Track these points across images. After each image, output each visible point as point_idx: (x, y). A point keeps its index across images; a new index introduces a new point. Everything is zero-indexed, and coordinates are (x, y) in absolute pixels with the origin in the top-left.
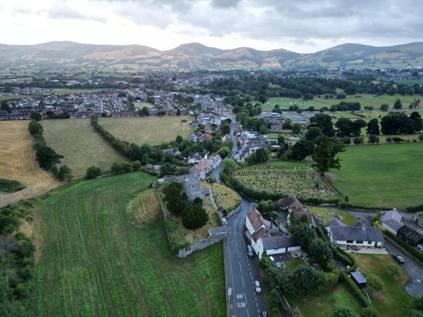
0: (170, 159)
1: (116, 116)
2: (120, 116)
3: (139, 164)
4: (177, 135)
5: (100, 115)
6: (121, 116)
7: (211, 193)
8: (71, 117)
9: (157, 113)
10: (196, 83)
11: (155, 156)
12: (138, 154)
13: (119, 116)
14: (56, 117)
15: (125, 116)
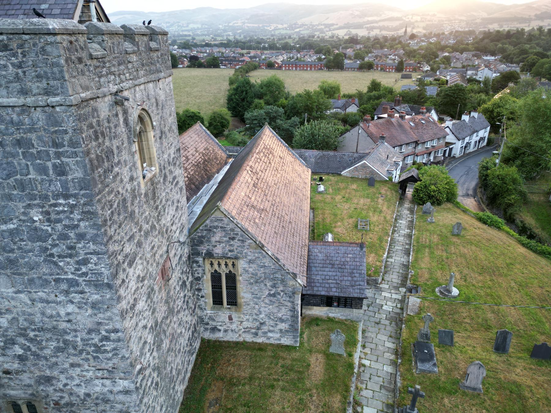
1: (289, 68)
3: (223, 118)
4: (371, 79)
6: (296, 69)
7: (394, 277)
8: (221, 67)
9: (358, 67)
10: (450, 41)
12: (243, 100)
13: (292, 68)
14: (200, 66)
15: (303, 70)
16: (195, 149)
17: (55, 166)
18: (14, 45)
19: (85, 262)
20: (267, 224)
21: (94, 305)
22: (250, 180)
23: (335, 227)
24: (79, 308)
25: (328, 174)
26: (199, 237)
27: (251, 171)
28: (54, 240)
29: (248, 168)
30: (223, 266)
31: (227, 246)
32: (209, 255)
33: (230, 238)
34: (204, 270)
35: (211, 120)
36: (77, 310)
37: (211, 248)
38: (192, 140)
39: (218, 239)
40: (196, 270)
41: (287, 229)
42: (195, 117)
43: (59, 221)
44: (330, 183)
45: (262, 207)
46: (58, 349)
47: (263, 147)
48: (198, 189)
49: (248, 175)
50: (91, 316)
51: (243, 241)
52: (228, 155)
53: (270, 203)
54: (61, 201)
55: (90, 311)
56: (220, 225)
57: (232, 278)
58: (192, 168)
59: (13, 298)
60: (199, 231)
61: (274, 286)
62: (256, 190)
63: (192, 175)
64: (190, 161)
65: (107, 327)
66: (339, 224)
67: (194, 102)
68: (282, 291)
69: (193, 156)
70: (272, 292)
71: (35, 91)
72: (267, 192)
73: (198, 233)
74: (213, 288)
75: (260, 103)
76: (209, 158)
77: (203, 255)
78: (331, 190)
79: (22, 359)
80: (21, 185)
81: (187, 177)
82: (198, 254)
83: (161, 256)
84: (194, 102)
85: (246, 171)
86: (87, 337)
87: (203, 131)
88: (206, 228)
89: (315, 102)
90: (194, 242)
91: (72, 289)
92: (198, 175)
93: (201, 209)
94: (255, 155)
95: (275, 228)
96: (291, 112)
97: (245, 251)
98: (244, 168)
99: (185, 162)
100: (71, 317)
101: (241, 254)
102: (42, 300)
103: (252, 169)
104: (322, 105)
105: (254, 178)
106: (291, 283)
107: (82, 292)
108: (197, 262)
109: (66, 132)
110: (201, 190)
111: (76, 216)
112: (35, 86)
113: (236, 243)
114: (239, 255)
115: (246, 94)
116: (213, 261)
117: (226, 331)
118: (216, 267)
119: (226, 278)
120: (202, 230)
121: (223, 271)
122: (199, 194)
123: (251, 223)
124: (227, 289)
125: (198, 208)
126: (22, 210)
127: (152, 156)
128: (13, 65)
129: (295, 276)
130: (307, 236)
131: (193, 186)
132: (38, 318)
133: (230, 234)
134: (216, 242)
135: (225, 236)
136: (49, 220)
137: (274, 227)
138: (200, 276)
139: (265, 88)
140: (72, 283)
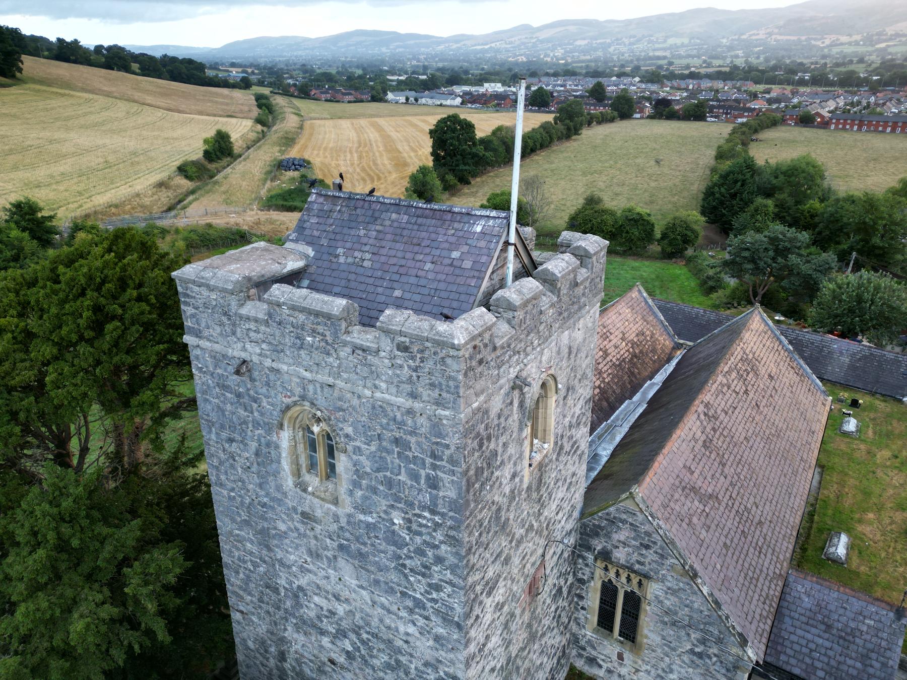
0: (876, 241)
1: (844, 126)
2: (856, 128)
3: (688, 228)
5: (791, 120)
6: (860, 129)
8: (709, 119)
11: (817, 219)
12: (733, 196)
14: (672, 116)
15: (876, 131)
16: (621, 335)
17: (428, 477)
18: (415, 349)
19: (438, 588)
20: (713, 527)
21: (437, 638)
22: (699, 433)
23: (860, 521)
24: (420, 633)
25: (873, 394)
26: (594, 525)
27: (705, 414)
28: (409, 551)
29: (701, 408)
30: (623, 579)
31: (636, 554)
32: (605, 556)
33: (641, 544)
34: (593, 574)
35: (667, 229)
36: (417, 635)
37: (609, 547)
38: (620, 318)
39: (622, 538)
40: (581, 569)
41: (750, 538)
42: (641, 222)
43: (420, 534)
44: (872, 415)
45: (710, 490)
46: (388, 666)
47: (739, 357)
48: (613, 409)
49: (698, 423)
51: (662, 556)
52: (676, 343)
53: (728, 482)
54: (426, 514)
55: (431, 643)
56: (630, 520)
57: (633, 603)
58: (610, 371)
59: (355, 591)
60: (595, 516)
61: (703, 641)
62: (708, 453)
63: (608, 383)
64: (608, 359)
65: (446, 669)
66: (871, 516)
67: (646, 186)
68: (715, 655)
69: (616, 347)
70: (697, 650)
71: (425, 398)
72: (726, 456)
73: (595, 519)
74: (601, 602)
75: (766, 206)
76: (641, 352)
77: (596, 552)
78: (870, 433)
79: (349, 656)
80: (389, 483)
81: (599, 387)
82: (589, 548)
83: (533, 564)
84: (646, 186)
85: (696, 415)
86: (422, 668)
87: (642, 299)
88: (607, 517)
89: (882, 218)
90: (585, 529)
91: (417, 610)
92: (616, 384)
93: (609, 452)
94: (720, 378)
95: (726, 537)
96: (827, 227)
97: (664, 572)
98: (693, 409)
99: (600, 360)
100: (409, 639)
101: (655, 573)
102: (383, 607)
103: (709, 409)
104: (896, 224)
105: (708, 430)
106: (735, 650)
108: (584, 558)
109: (447, 447)
110: (617, 412)
111: (439, 536)
112: (426, 393)
113: (650, 555)
114: (652, 573)
115: (742, 185)
116: (610, 566)
117: (609, 671)
118: (612, 575)
119: (625, 597)
120: (601, 517)
121: (623, 587)
122: (612, 418)
123: (684, 525)
124: (623, 612)
125: (605, 449)
126: (385, 508)
127: (547, 429)
128: (409, 367)
129: (744, 642)
130: (788, 555)
131: (605, 404)
132: (375, 622)
133: (643, 539)
134: (620, 541)
135: (634, 539)
136: (409, 529)
137: (725, 533)
138: (585, 578)
139: (782, 177)
140: (419, 604)
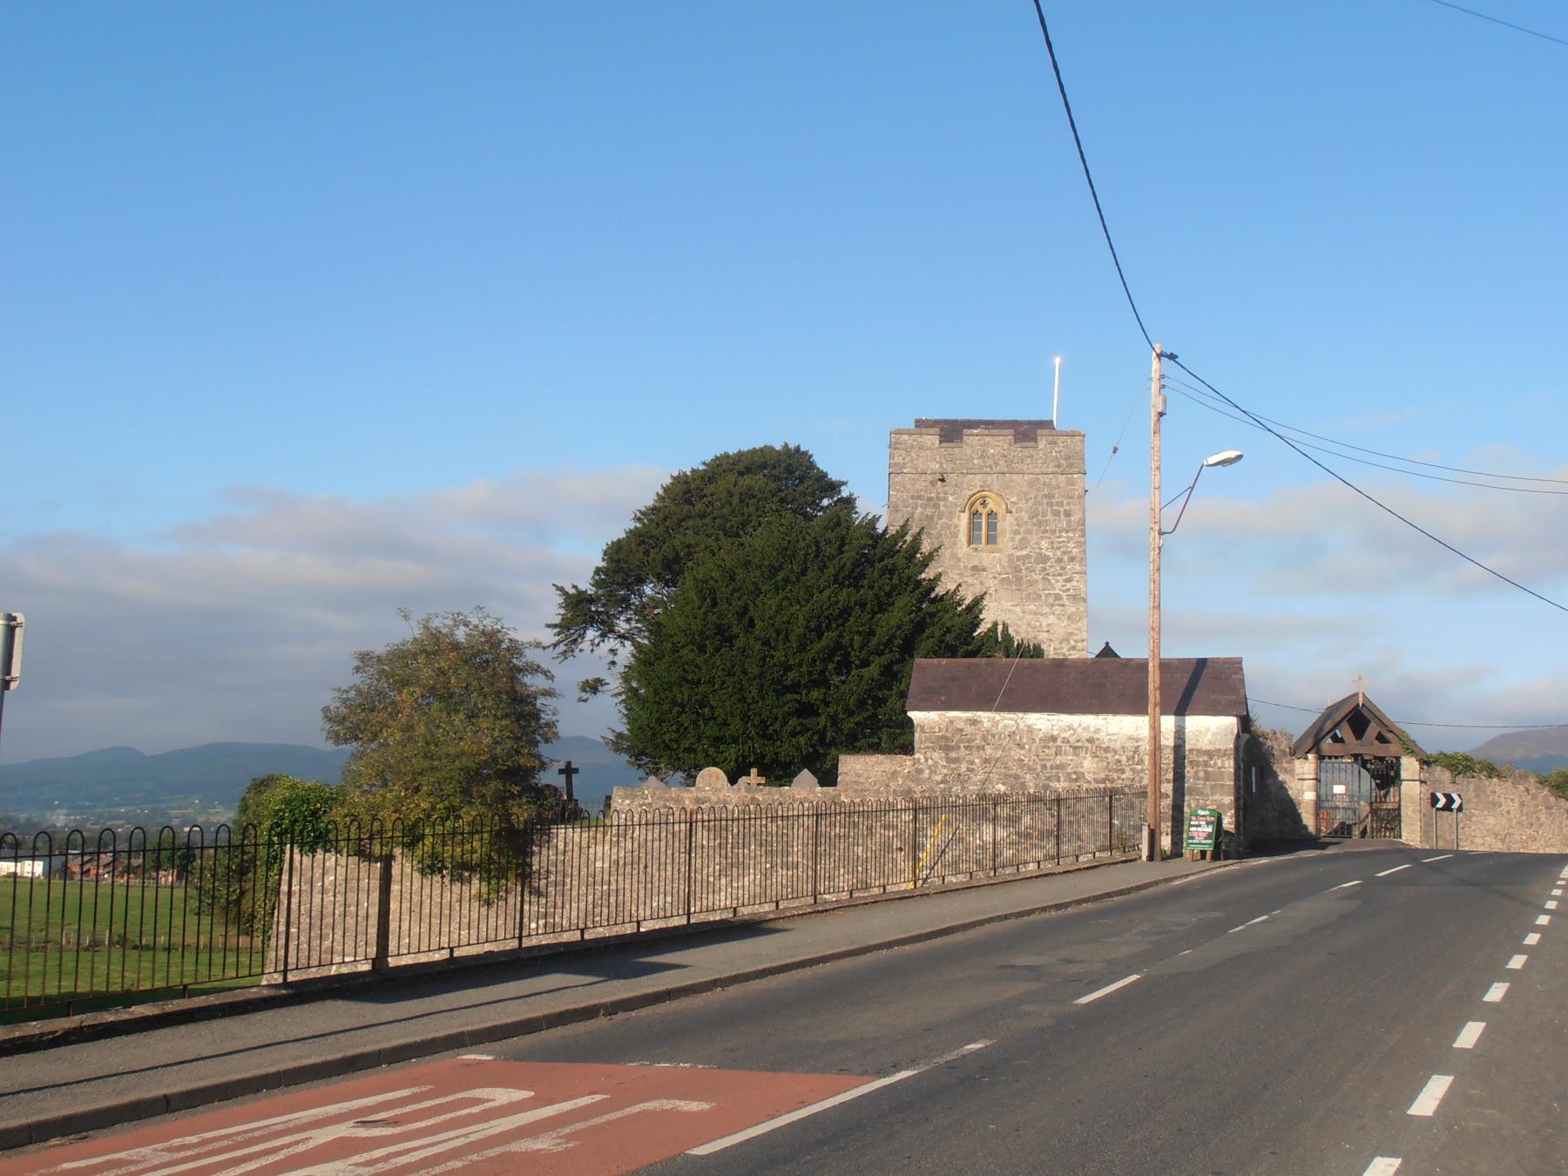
17: (1065, 511)
19: (1069, 580)
36: (1056, 621)
43: (1058, 548)
50: (1065, 627)
54: (1064, 534)
55: (1065, 623)
59: (1009, 611)
65: (1075, 638)
91: (1056, 602)
100: (1050, 628)
102: (1031, 613)
107: (1063, 606)
111: (1071, 545)
128: (1056, 452)
136: (1052, 548)
140: (1057, 597)
